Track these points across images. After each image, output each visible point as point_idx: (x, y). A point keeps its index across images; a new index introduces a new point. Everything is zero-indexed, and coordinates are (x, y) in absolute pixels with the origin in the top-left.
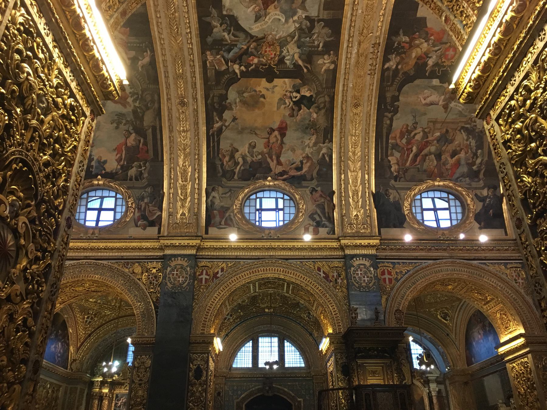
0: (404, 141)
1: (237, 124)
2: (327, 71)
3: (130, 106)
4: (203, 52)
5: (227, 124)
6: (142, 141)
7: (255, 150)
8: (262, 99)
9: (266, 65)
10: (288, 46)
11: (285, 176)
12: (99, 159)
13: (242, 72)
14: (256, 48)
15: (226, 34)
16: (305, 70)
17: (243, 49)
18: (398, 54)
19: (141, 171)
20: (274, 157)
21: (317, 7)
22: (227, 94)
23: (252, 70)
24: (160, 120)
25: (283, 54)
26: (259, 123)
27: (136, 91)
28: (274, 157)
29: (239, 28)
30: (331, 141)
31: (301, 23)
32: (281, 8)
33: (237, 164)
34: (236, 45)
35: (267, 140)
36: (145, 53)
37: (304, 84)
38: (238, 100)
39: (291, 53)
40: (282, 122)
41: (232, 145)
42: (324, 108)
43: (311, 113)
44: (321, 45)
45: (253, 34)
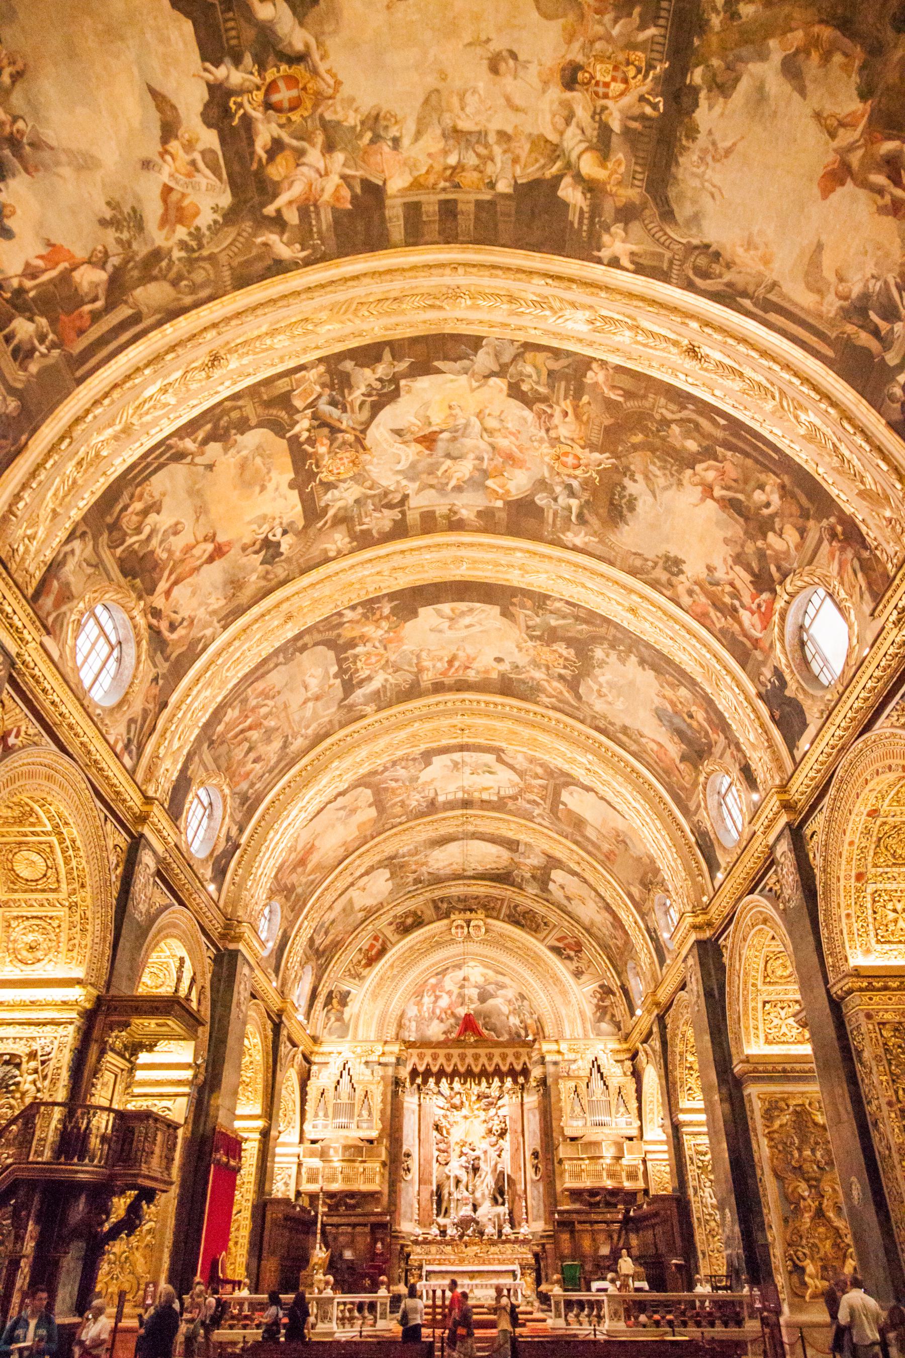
0: (253, 702)
1: (204, 476)
2: (326, 551)
3: (167, 239)
4: (320, 360)
5: (198, 460)
6: (99, 304)
7: (172, 538)
8: (257, 489)
9: (318, 466)
10: (356, 487)
11: (154, 622)
12: (7, 211)
13: (297, 436)
14: (344, 443)
15: (363, 389)
16: (320, 524)
17: (338, 424)
18: (364, 615)
19: (33, 350)
20: (173, 577)
21: (426, 503)
22: (251, 428)
23: (305, 451)
24: (159, 324)
25: (341, 485)
26: (216, 510)
27: (205, 241)
28: (173, 577)
29: (376, 408)
30: (225, 628)
31: (396, 491)
32: (418, 461)
33: (138, 530)
34: (344, 410)
35: (193, 542)
36: (298, 246)
37: (298, 534)
38: (244, 453)
39: (345, 495)
40: (229, 544)
41: (164, 494)
42: (269, 580)
43: (254, 570)
44: (364, 527)
45: (368, 432)
